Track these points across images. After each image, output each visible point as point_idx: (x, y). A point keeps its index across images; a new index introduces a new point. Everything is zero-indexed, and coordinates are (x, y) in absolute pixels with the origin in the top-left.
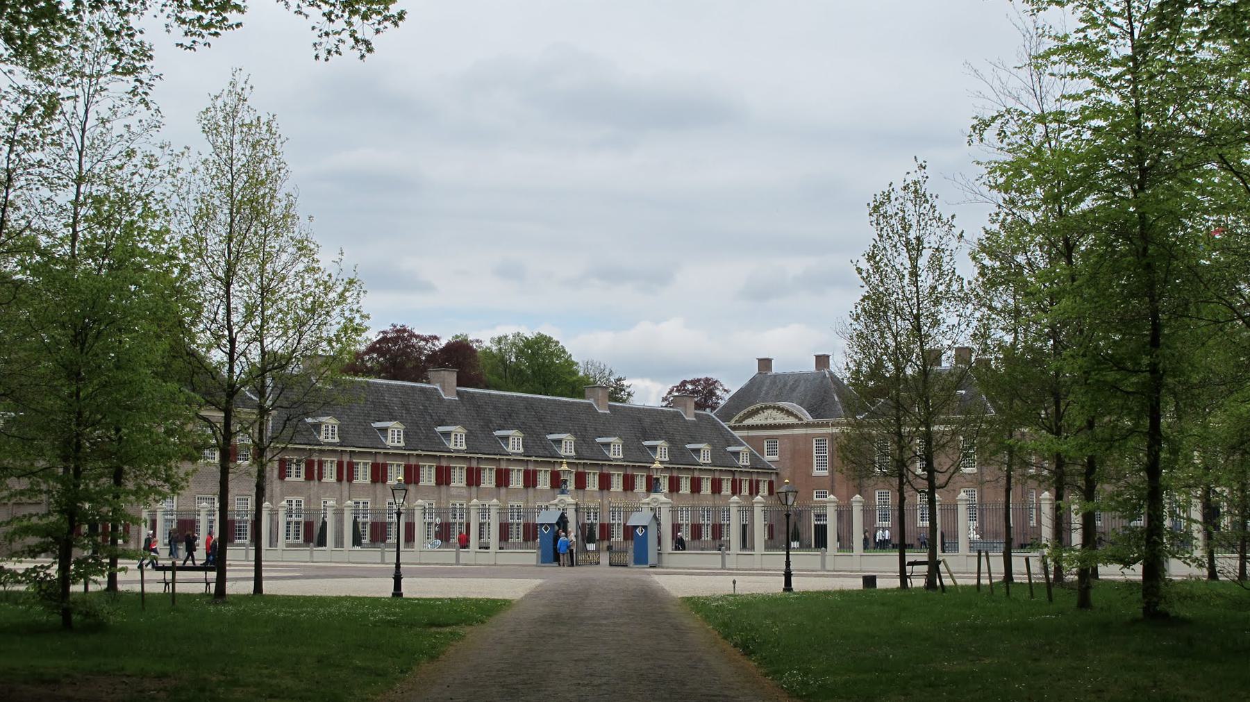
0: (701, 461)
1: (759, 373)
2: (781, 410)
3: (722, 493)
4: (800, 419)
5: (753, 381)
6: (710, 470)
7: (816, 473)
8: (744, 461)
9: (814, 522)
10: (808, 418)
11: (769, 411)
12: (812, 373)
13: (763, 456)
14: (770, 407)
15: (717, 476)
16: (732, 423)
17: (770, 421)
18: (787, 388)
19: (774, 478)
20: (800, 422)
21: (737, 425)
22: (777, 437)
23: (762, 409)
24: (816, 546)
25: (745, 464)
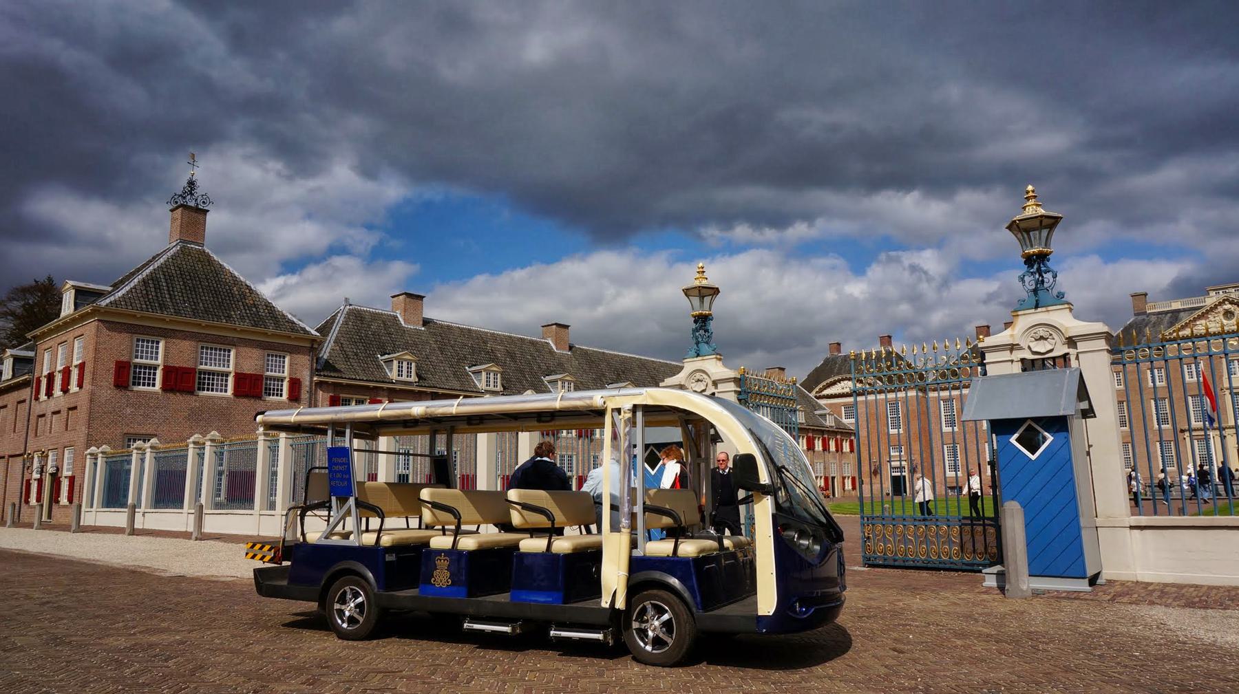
5: (827, 361)
11: (846, 382)
16: (814, 392)
19: (853, 438)
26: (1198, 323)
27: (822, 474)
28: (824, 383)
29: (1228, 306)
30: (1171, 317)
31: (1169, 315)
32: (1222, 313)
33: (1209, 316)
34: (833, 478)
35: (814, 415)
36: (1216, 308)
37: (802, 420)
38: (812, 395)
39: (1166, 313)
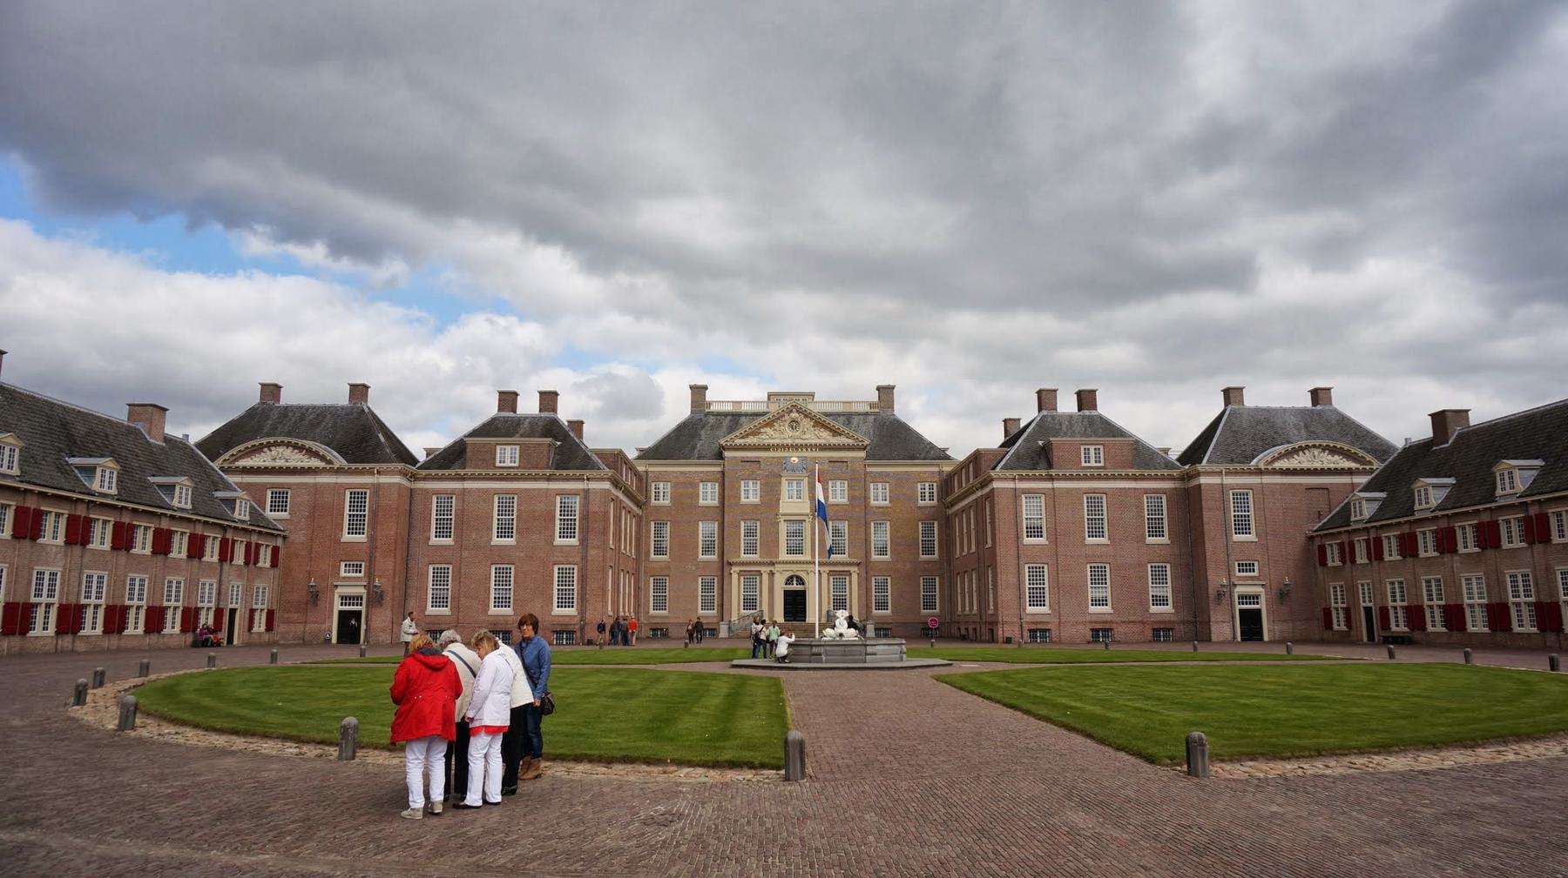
0: (175, 503)
1: (262, 403)
2: (301, 448)
3: (205, 559)
4: (330, 462)
5: (251, 413)
6: (189, 520)
7: (347, 537)
8: (241, 514)
9: (338, 606)
10: (339, 461)
11: (281, 449)
12: (342, 408)
13: (264, 509)
14: (282, 444)
15: (199, 530)
17: (280, 463)
18: (306, 422)
19: (279, 542)
20: (328, 467)
21: (226, 465)
22: (289, 486)
23: (269, 446)
24: (340, 640)
25: (242, 518)
26: (762, 430)
27: (213, 605)
28: (241, 447)
29: (794, 415)
30: (731, 421)
31: (729, 417)
32: (789, 421)
33: (775, 424)
34: (233, 611)
35: (212, 498)
36: (784, 416)
37: (186, 503)
38: (215, 465)
39: (726, 415)
